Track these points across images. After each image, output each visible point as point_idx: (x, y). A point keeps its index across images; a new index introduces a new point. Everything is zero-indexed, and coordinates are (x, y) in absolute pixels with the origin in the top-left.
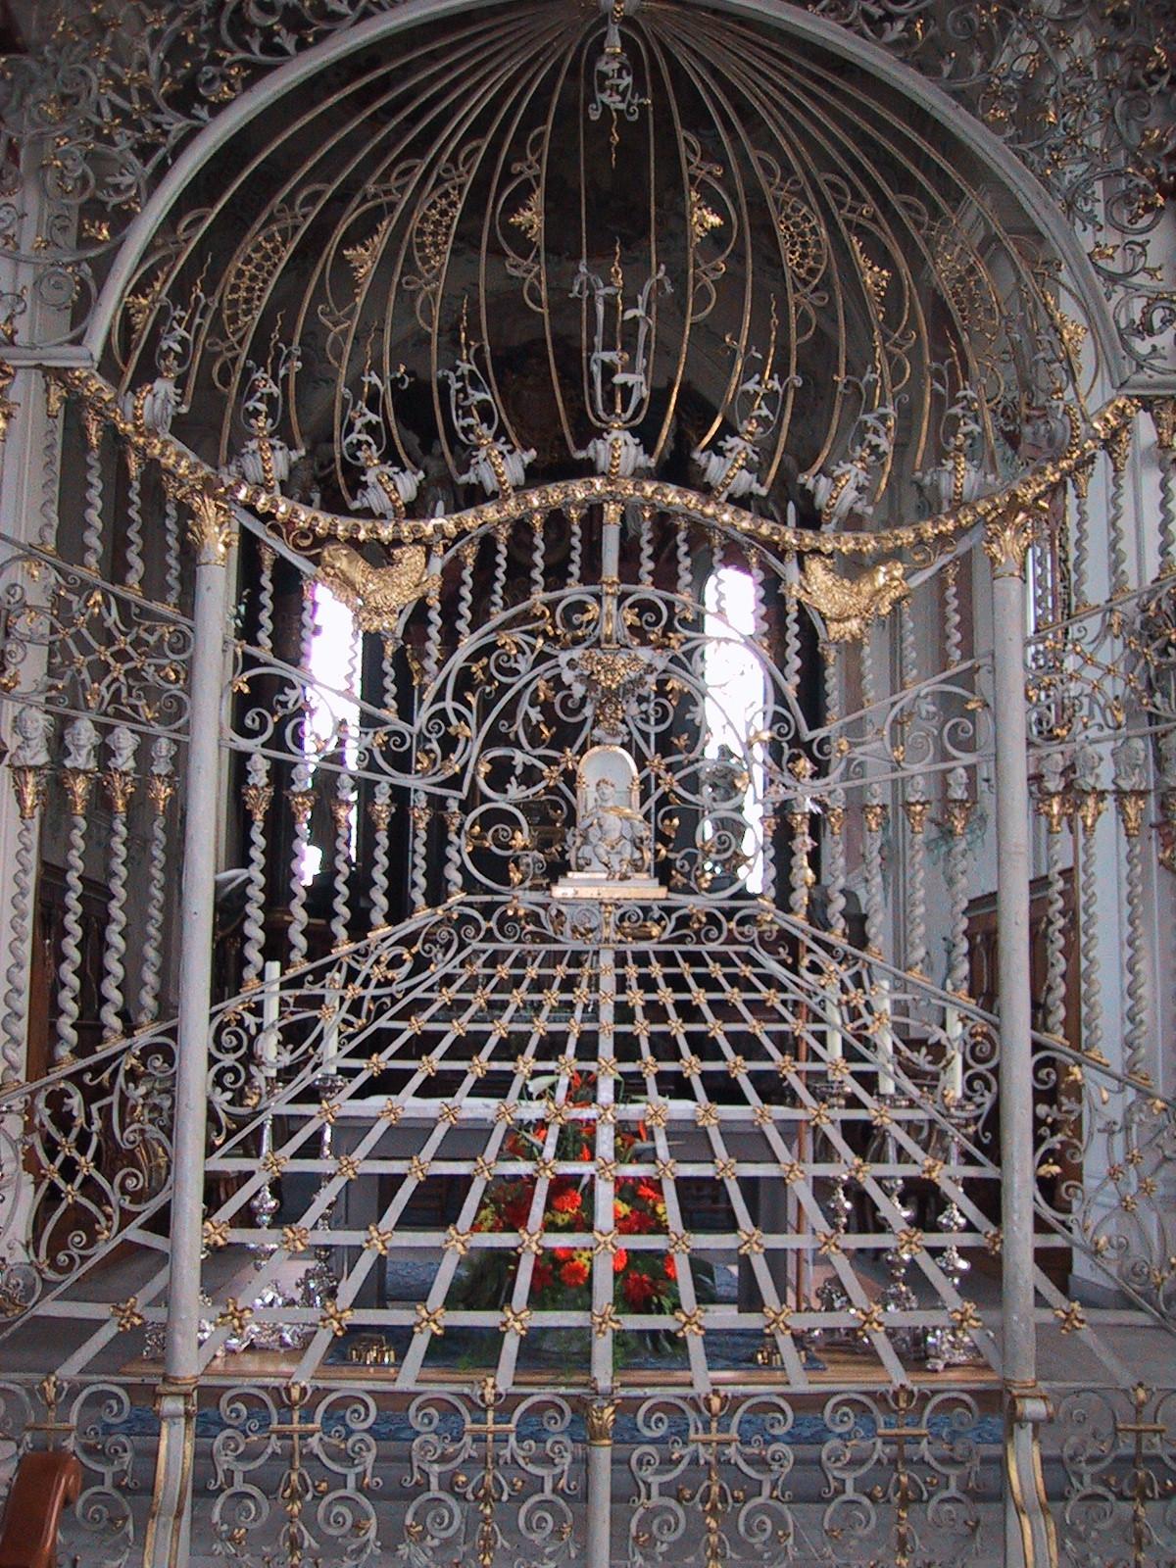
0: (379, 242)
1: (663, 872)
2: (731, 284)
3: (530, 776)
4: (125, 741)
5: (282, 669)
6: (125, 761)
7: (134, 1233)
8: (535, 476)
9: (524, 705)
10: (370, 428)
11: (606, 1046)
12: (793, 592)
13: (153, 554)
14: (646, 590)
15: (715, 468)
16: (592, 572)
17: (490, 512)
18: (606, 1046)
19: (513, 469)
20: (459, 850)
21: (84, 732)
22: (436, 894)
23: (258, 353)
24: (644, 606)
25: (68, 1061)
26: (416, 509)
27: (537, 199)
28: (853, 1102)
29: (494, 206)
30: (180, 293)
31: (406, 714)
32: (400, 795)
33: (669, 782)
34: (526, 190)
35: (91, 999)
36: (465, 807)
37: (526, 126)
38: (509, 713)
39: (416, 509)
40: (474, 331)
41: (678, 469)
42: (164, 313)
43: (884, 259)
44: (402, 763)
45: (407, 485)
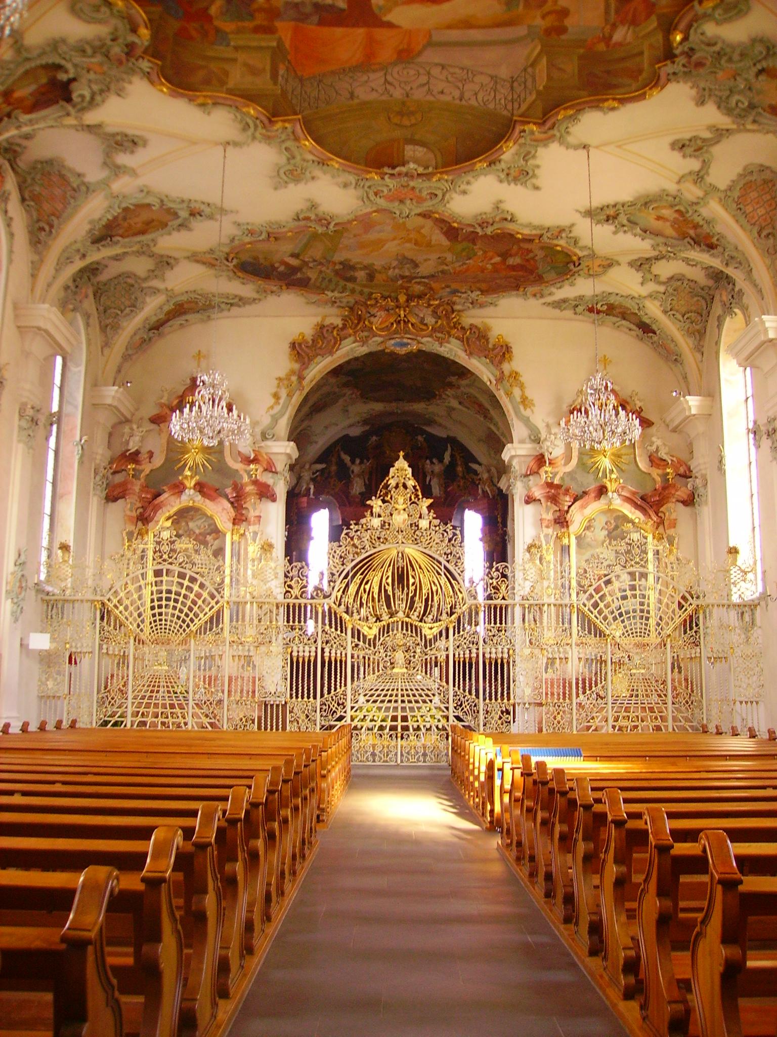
2: (415, 590)
4: (339, 652)
6: (339, 655)
7: (342, 714)
13: (341, 627)
14: (404, 631)
17: (384, 623)
19: (387, 618)
20: (381, 666)
21: (333, 652)
27: (390, 579)
30: (343, 592)
35: (335, 685)
41: (408, 616)
45: (374, 619)
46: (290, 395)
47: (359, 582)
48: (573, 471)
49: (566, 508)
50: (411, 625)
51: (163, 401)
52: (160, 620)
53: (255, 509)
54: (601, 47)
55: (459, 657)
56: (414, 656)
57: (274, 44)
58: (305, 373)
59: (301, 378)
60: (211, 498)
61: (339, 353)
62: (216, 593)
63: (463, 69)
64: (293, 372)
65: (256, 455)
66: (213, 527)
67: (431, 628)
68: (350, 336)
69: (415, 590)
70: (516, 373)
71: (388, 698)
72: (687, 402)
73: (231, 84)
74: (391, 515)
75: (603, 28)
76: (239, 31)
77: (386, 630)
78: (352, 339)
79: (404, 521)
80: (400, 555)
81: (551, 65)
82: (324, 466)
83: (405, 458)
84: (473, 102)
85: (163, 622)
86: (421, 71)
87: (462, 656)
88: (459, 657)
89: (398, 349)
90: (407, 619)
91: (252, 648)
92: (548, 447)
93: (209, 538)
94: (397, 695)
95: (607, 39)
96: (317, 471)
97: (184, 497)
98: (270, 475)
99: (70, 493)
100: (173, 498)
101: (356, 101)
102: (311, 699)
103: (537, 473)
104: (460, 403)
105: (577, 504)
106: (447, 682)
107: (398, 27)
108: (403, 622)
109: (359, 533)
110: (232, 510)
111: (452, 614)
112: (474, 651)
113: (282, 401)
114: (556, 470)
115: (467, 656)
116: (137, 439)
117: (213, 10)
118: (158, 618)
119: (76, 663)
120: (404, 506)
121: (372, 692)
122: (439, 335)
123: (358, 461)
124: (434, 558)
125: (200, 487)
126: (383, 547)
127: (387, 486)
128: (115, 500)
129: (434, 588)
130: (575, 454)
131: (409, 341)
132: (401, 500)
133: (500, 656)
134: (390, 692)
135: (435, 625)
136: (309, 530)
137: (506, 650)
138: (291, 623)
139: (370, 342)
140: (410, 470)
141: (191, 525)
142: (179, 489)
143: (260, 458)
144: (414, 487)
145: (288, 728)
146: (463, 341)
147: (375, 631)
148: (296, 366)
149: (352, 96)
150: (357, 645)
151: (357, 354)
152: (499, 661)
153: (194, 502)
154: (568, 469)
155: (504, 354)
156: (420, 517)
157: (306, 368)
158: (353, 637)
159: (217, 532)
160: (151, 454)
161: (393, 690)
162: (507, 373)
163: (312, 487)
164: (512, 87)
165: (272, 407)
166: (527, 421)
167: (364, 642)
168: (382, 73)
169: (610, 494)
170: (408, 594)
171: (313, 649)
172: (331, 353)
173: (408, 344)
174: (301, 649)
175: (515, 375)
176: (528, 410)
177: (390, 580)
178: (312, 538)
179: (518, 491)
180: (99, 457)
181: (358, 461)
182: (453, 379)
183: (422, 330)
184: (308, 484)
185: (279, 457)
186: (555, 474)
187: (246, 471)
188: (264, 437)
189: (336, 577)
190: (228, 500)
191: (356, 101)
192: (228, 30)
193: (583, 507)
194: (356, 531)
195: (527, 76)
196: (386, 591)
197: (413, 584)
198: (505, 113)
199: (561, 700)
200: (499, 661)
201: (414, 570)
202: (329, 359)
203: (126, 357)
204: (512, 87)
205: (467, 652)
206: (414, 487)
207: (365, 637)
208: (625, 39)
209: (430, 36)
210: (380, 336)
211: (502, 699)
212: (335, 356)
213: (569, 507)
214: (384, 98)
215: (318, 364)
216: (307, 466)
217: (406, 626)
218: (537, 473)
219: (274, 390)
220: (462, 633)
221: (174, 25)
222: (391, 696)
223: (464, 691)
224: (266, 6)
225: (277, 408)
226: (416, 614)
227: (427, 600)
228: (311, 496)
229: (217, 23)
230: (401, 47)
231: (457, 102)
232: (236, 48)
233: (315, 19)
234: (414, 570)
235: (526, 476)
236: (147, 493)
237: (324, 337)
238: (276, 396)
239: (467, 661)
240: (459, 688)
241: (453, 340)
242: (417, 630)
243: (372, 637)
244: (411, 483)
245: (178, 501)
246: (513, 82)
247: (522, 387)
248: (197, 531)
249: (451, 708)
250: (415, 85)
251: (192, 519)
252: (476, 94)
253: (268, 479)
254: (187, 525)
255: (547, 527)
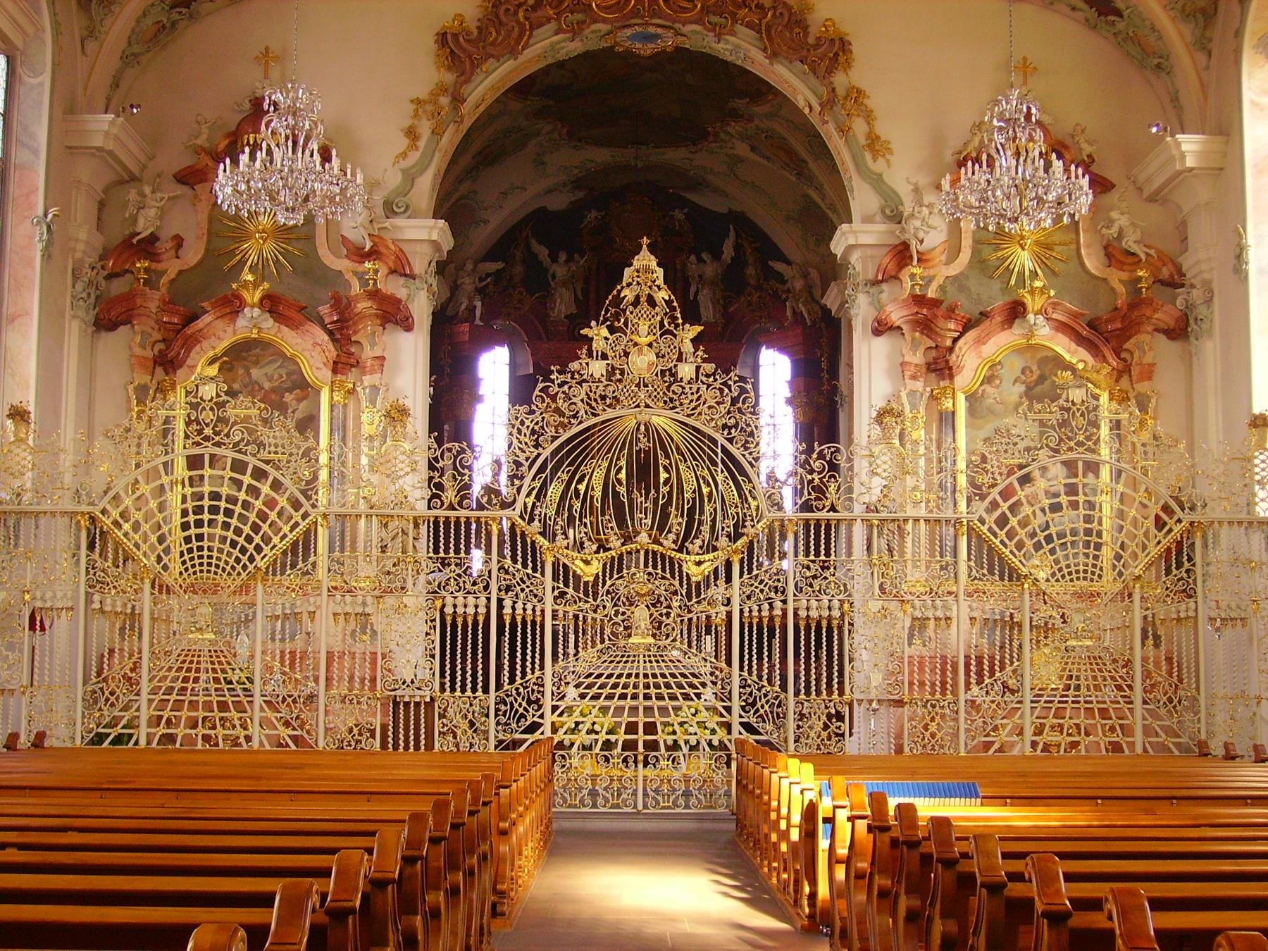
0: (585, 484)
1: (654, 636)
2: (670, 493)
3: (624, 614)
4: (529, 606)
5: (566, 590)
6: (529, 612)
7: (536, 719)
8: (623, 544)
9: (622, 598)
10: (585, 533)
11: (641, 675)
12: (685, 570)
14: (650, 569)
15: (665, 543)
16: (637, 566)
18: (641, 675)
19: (618, 543)
20: (607, 631)
21: (519, 606)
22: (603, 641)
23: (557, 513)
24: (649, 574)
25: (519, 681)
26: (597, 552)
27: (624, 471)
28: (722, 715)
29: (613, 474)
30: (538, 498)
31: (595, 600)
32: (594, 620)
33: (656, 614)
34: (621, 468)
35: (524, 666)
36: (609, 621)
37: (620, 451)
38: (618, 599)
39: (597, 552)
40: (609, 508)
41: (656, 542)
42: (534, 504)
43: (709, 485)
44: (595, 611)
45: (595, 547)
46: (437, 133)
47: (565, 477)
48: (962, 273)
49: (949, 343)
50: (663, 556)
51: (199, 142)
52: (200, 549)
53: (373, 345)
55: (751, 617)
56: (668, 615)
58: (465, 90)
59: (458, 100)
60: (293, 325)
61: (529, 53)
62: (302, 499)
64: (441, 89)
65: (375, 245)
66: (295, 377)
67: (699, 563)
68: (549, 20)
69: (670, 493)
70: (859, 91)
71: (619, 691)
72: (1178, 144)
74: (627, 354)
77: (616, 566)
78: (553, 26)
79: (650, 365)
80: (642, 428)
82: (499, 265)
83: (652, 249)
85: (206, 553)
87: (755, 614)
88: (751, 617)
89: (639, 45)
90: (656, 547)
91: (369, 600)
92: (916, 229)
93: (288, 398)
94: (635, 687)
96: (488, 275)
97: (241, 322)
98: (402, 280)
99: (28, 313)
100: (220, 324)
102: (479, 693)
103: (896, 278)
104: (753, 149)
105: (971, 335)
106: (729, 663)
108: (647, 552)
109: (566, 388)
110: (331, 346)
111: (737, 536)
112: (778, 604)
113: (422, 144)
114: (932, 272)
115: (765, 613)
116: (152, 212)
118: (195, 544)
119: (43, 629)
120: (651, 338)
121: (591, 679)
122: (715, 19)
123: (563, 257)
124: (703, 434)
125: (272, 304)
126: (610, 414)
127: (618, 300)
128: (112, 326)
129: (705, 490)
130: (967, 243)
131: (659, 31)
132: (644, 328)
133: (825, 613)
134: (623, 680)
135: (707, 557)
136: (475, 382)
137: (836, 603)
138: (442, 555)
139: (587, 32)
140: (660, 272)
141: (256, 373)
142: (232, 306)
143: (383, 250)
144: (669, 303)
145: (437, 745)
146: (759, 32)
147: (596, 567)
148: (449, 78)
150: (563, 594)
151: (562, 55)
152: (824, 623)
153: (260, 330)
154: (953, 270)
155: (836, 54)
156: (680, 359)
157: (467, 81)
158: (555, 578)
159: (304, 388)
160: (179, 242)
161: (629, 676)
162: (841, 92)
163: (479, 304)
165: (404, 155)
166: (877, 182)
167: (576, 589)
169: (1031, 317)
170: (656, 501)
171: (483, 601)
172: (514, 53)
173: (657, 36)
174: (460, 601)
175: (857, 95)
176: (880, 160)
177: (623, 476)
178: (479, 399)
179: (861, 311)
180: (81, 247)
181: (563, 257)
182: (740, 103)
183: (685, 10)
184: (471, 299)
185: (418, 248)
186: (930, 280)
187: (355, 273)
188: (390, 209)
189: (523, 469)
190: (324, 327)
193: (980, 341)
194: (560, 386)
196: (616, 494)
197: (666, 483)
199: (938, 696)
200: (824, 623)
201: (667, 457)
202: (509, 65)
203: (130, 59)
205: (766, 606)
206: (669, 303)
207: (577, 578)
210: (604, 21)
211: (830, 693)
212: (521, 59)
213: (955, 340)
215: (488, 73)
216: (470, 267)
217: (653, 558)
218: (896, 278)
219: (407, 123)
220: (755, 572)
222: (625, 686)
223: (760, 677)
225: (414, 157)
226: (672, 536)
227: (691, 511)
228: (478, 322)
234: (667, 457)
235: (876, 283)
236: (173, 313)
237: (501, 23)
238: (412, 134)
239: (765, 621)
240: (750, 674)
241: (739, 27)
242: (673, 567)
243: (592, 579)
244: (662, 295)
245: (230, 330)
247: (869, 116)
248: (267, 385)
249: (736, 710)
251: (256, 363)
253: (396, 288)
254: (249, 374)
255: (914, 378)
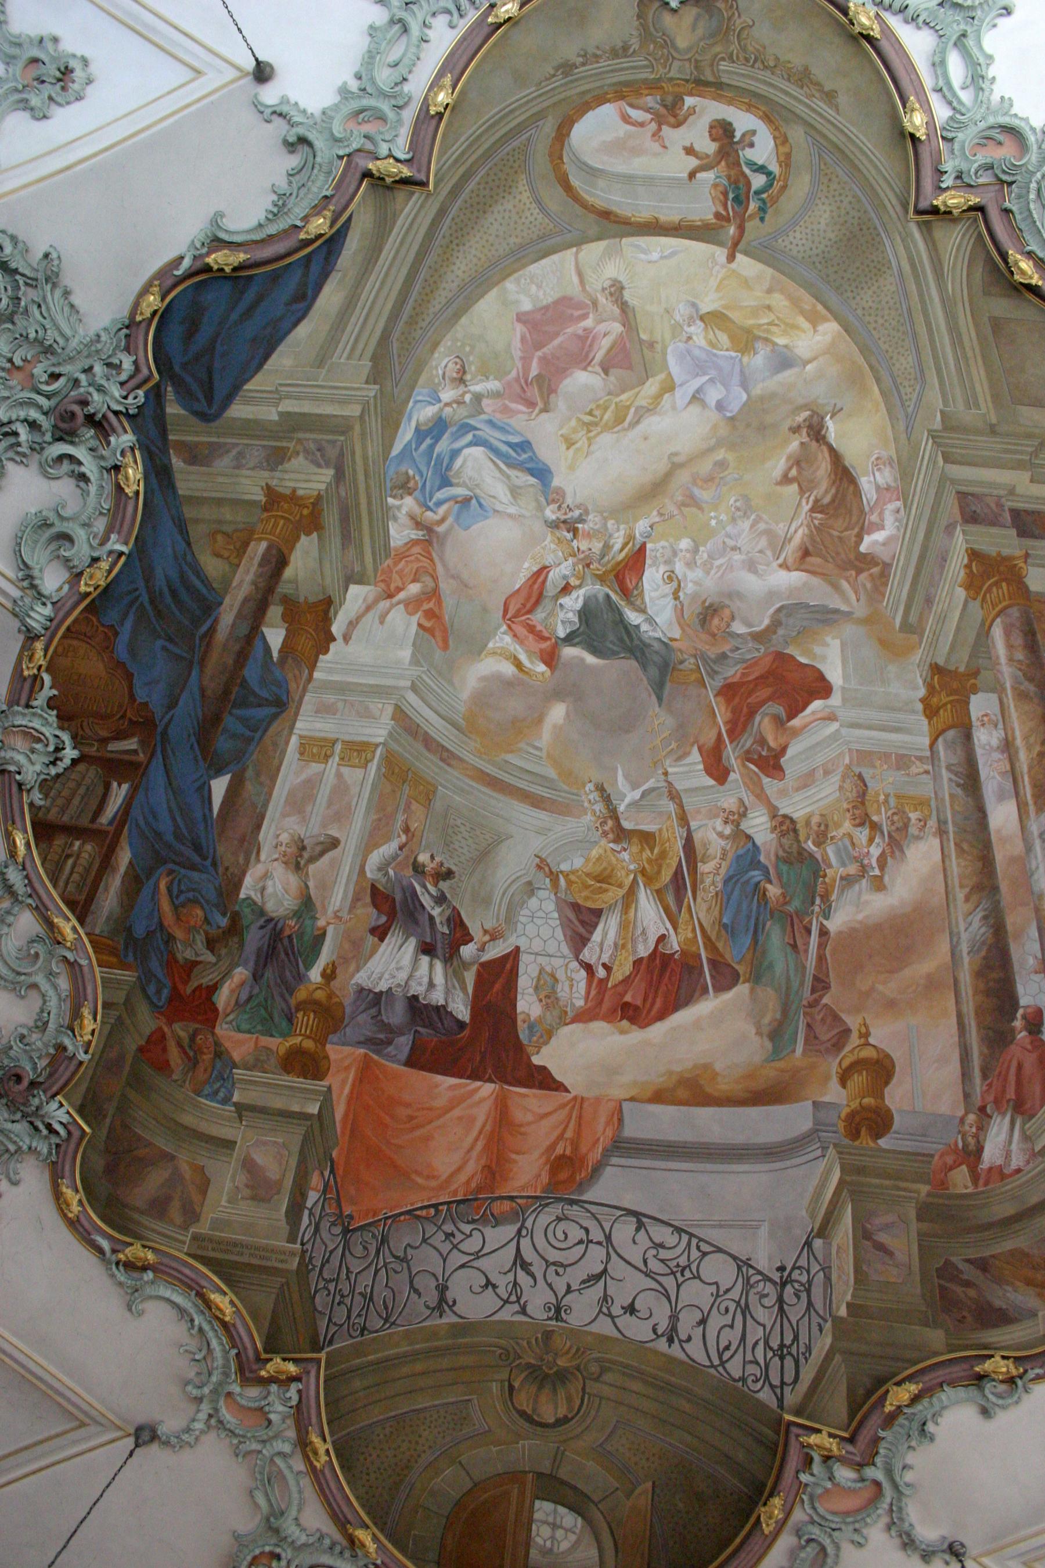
54: (960, 1179)
57: (314, 1109)
63: (679, 1230)
73: (203, 1228)
75: (962, 1120)
76: (256, 1064)
81: (863, 1234)
84: (696, 1350)
86: (597, 1235)
95: (972, 1155)
101: (449, 1319)
107: (559, 1087)
117: (223, 998)
149: (443, 1303)
164: (780, 1300)
168: (511, 1230)
191: (449, 1319)
192: (236, 1056)
195: (815, 1268)
198: (766, 1396)
204: (780, 1300)
208: (1008, 1155)
209: (621, 1120)
214: (507, 1314)
221: (147, 1021)
224: (320, 995)
229: (222, 1030)
230: (559, 1150)
231: (662, 1345)
232: (241, 1109)
233: (404, 1043)
246: (783, 1284)
250: (576, 1276)
252: (703, 1322)
